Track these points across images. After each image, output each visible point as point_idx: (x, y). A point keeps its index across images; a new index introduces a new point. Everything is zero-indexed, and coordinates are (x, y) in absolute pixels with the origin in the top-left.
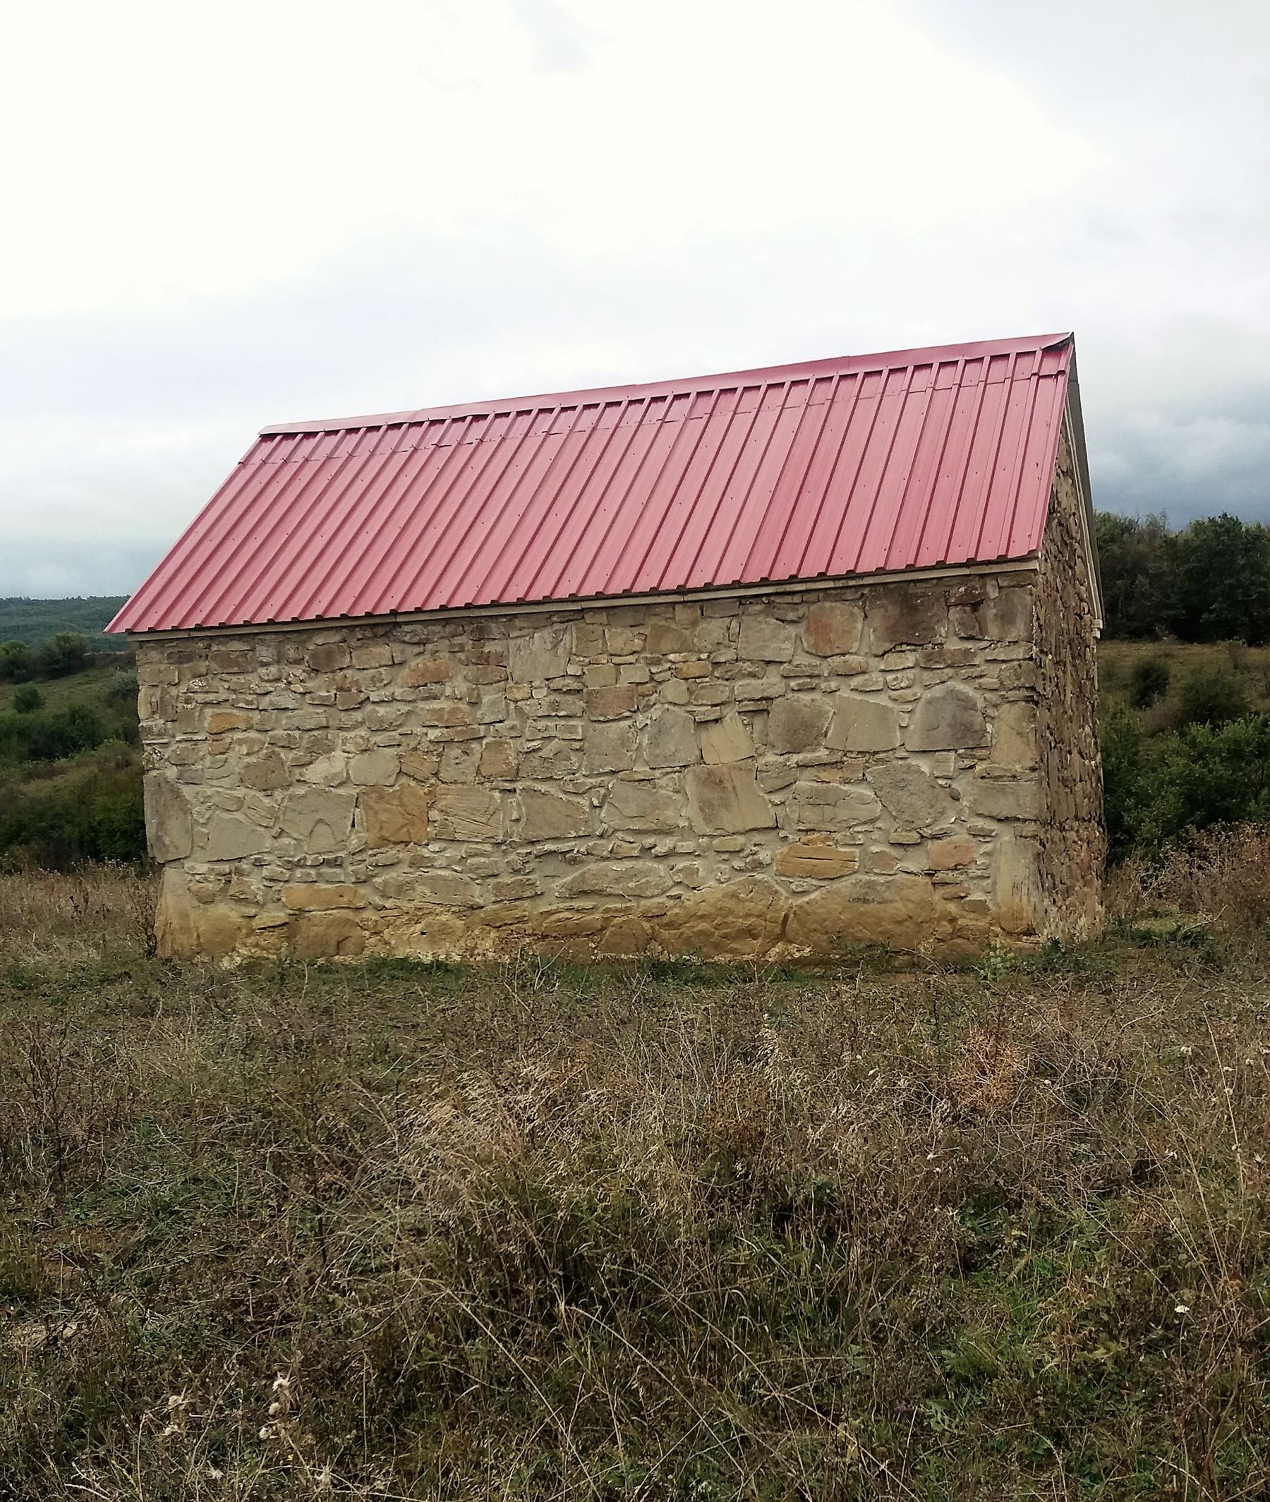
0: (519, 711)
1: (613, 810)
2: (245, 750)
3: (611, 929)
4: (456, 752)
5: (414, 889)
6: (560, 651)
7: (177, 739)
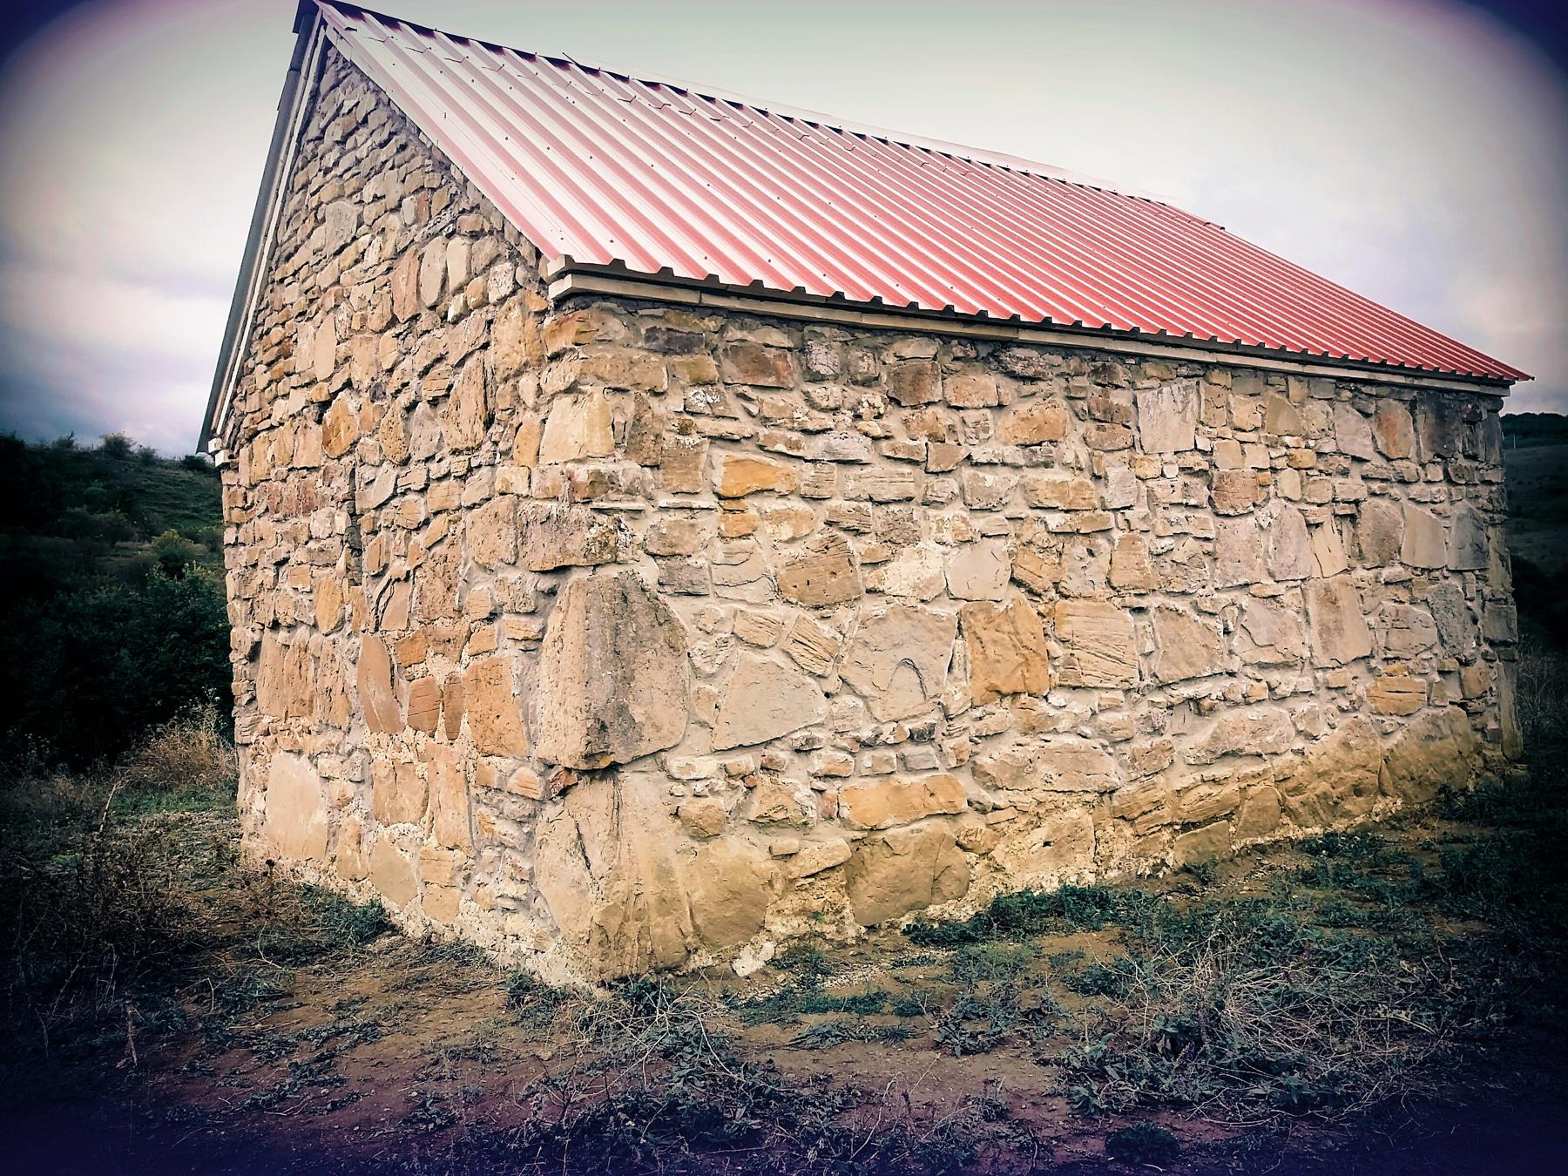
0: (1151, 494)
2: (786, 531)
4: (1080, 549)
5: (1035, 770)
6: (1189, 415)
7: (663, 503)
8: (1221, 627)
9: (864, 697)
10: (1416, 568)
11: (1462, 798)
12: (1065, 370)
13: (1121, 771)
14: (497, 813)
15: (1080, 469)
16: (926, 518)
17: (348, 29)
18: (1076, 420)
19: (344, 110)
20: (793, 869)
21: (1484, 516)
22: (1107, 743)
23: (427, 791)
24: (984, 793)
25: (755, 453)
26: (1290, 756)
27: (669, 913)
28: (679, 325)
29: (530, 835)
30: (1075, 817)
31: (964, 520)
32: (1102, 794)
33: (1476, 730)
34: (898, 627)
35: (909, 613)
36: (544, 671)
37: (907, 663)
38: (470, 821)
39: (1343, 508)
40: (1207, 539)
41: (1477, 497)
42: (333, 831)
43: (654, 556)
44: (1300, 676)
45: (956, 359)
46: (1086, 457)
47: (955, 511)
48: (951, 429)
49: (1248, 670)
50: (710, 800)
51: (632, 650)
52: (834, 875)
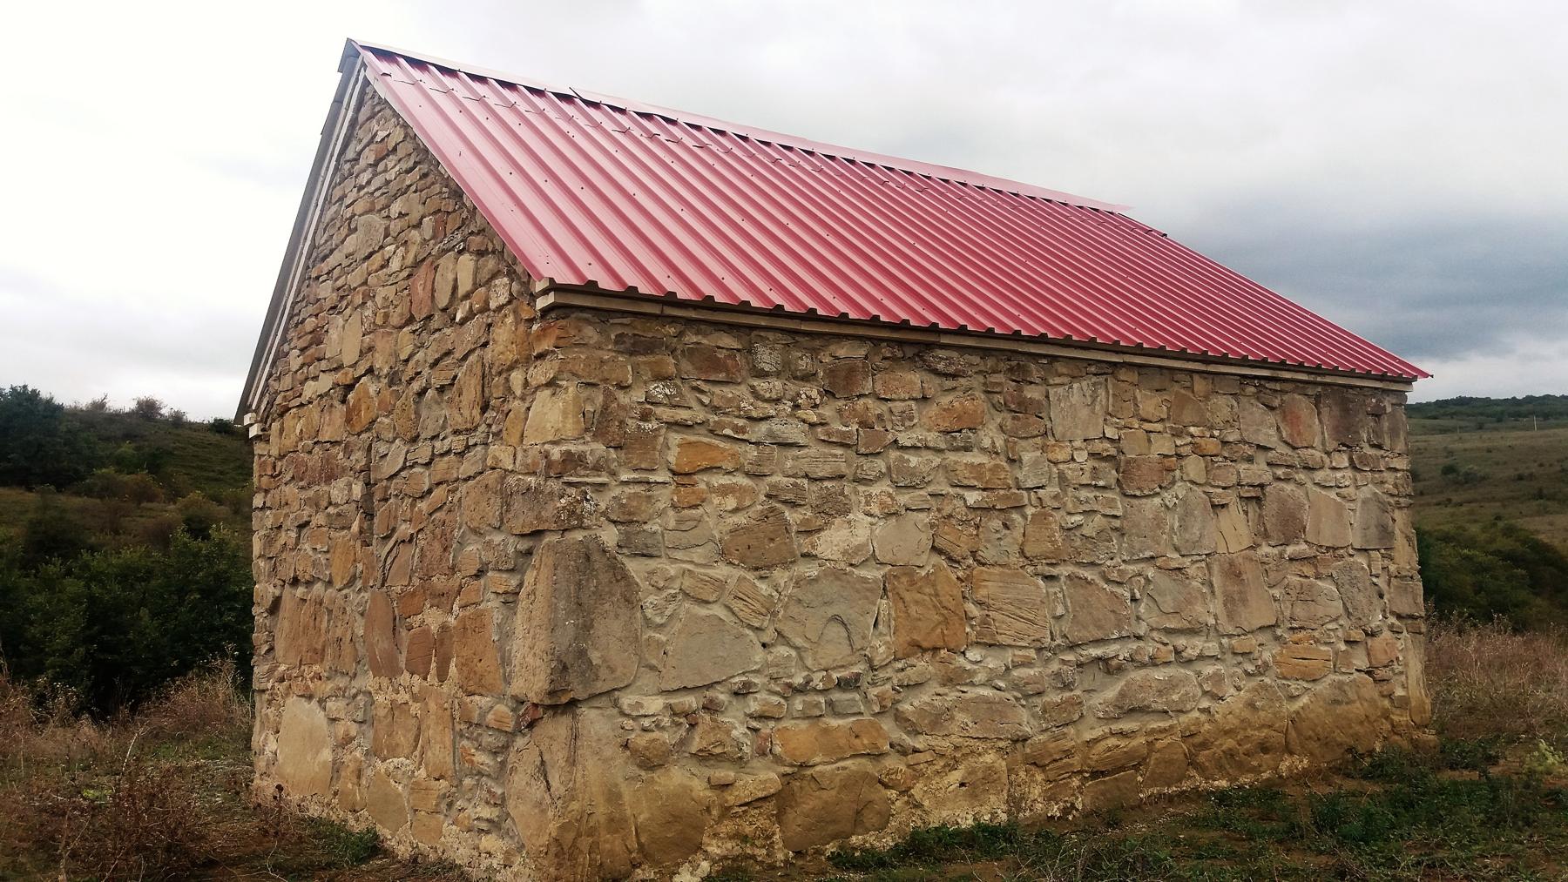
0: (1062, 476)
1: (1151, 604)
2: (731, 503)
3: (1155, 756)
4: (996, 524)
5: (952, 718)
7: (624, 477)
8: (1128, 595)
9: (797, 648)
10: (1321, 546)
11: (1368, 760)
12: (983, 368)
13: (1033, 722)
14: (476, 745)
15: (997, 453)
16: (856, 493)
17: (384, 74)
18: (993, 411)
19: (378, 139)
20: (729, 798)
21: (1392, 500)
22: (1020, 696)
23: (419, 728)
24: (904, 736)
25: (706, 436)
26: (1196, 714)
27: (616, 831)
28: (644, 331)
29: (503, 763)
30: (989, 761)
31: (890, 495)
32: (1015, 742)
33: (1383, 696)
34: (830, 588)
35: (838, 575)
36: (519, 618)
37: (836, 618)
38: (454, 753)
39: (1248, 491)
40: (1115, 517)
41: (1382, 482)
42: (337, 768)
43: (614, 522)
44: (1206, 642)
45: (885, 358)
46: (1002, 442)
47: (883, 487)
48: (880, 417)
49: (1155, 634)
50: (656, 734)
51: (591, 602)
52: (766, 804)
